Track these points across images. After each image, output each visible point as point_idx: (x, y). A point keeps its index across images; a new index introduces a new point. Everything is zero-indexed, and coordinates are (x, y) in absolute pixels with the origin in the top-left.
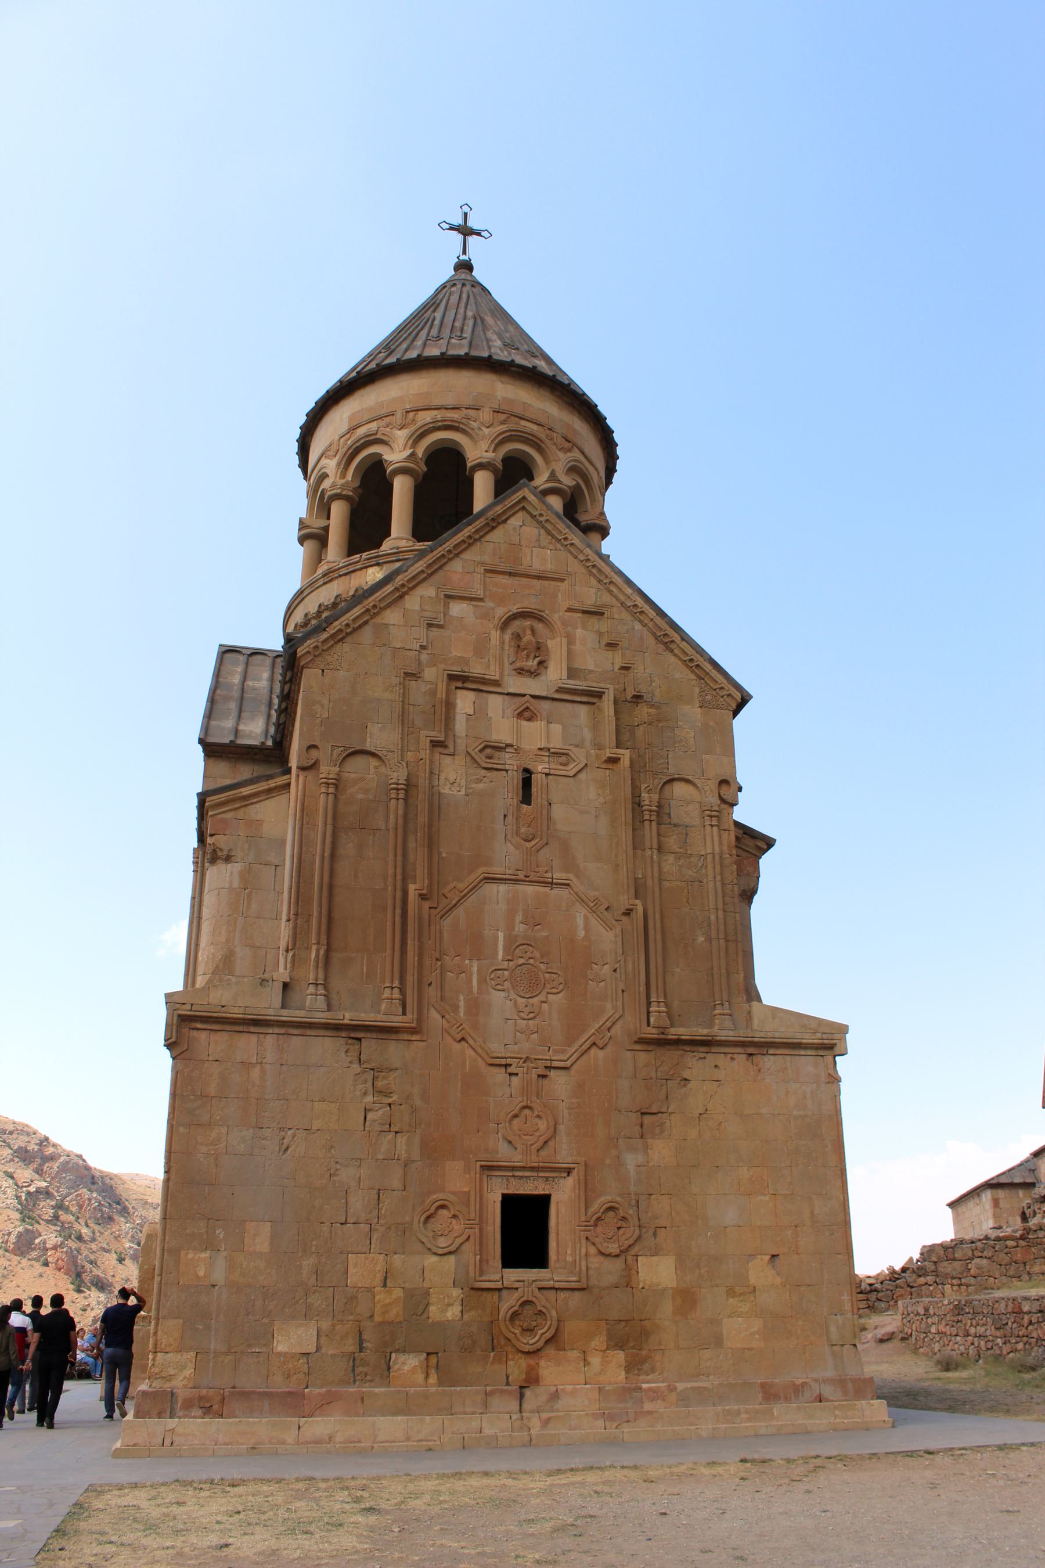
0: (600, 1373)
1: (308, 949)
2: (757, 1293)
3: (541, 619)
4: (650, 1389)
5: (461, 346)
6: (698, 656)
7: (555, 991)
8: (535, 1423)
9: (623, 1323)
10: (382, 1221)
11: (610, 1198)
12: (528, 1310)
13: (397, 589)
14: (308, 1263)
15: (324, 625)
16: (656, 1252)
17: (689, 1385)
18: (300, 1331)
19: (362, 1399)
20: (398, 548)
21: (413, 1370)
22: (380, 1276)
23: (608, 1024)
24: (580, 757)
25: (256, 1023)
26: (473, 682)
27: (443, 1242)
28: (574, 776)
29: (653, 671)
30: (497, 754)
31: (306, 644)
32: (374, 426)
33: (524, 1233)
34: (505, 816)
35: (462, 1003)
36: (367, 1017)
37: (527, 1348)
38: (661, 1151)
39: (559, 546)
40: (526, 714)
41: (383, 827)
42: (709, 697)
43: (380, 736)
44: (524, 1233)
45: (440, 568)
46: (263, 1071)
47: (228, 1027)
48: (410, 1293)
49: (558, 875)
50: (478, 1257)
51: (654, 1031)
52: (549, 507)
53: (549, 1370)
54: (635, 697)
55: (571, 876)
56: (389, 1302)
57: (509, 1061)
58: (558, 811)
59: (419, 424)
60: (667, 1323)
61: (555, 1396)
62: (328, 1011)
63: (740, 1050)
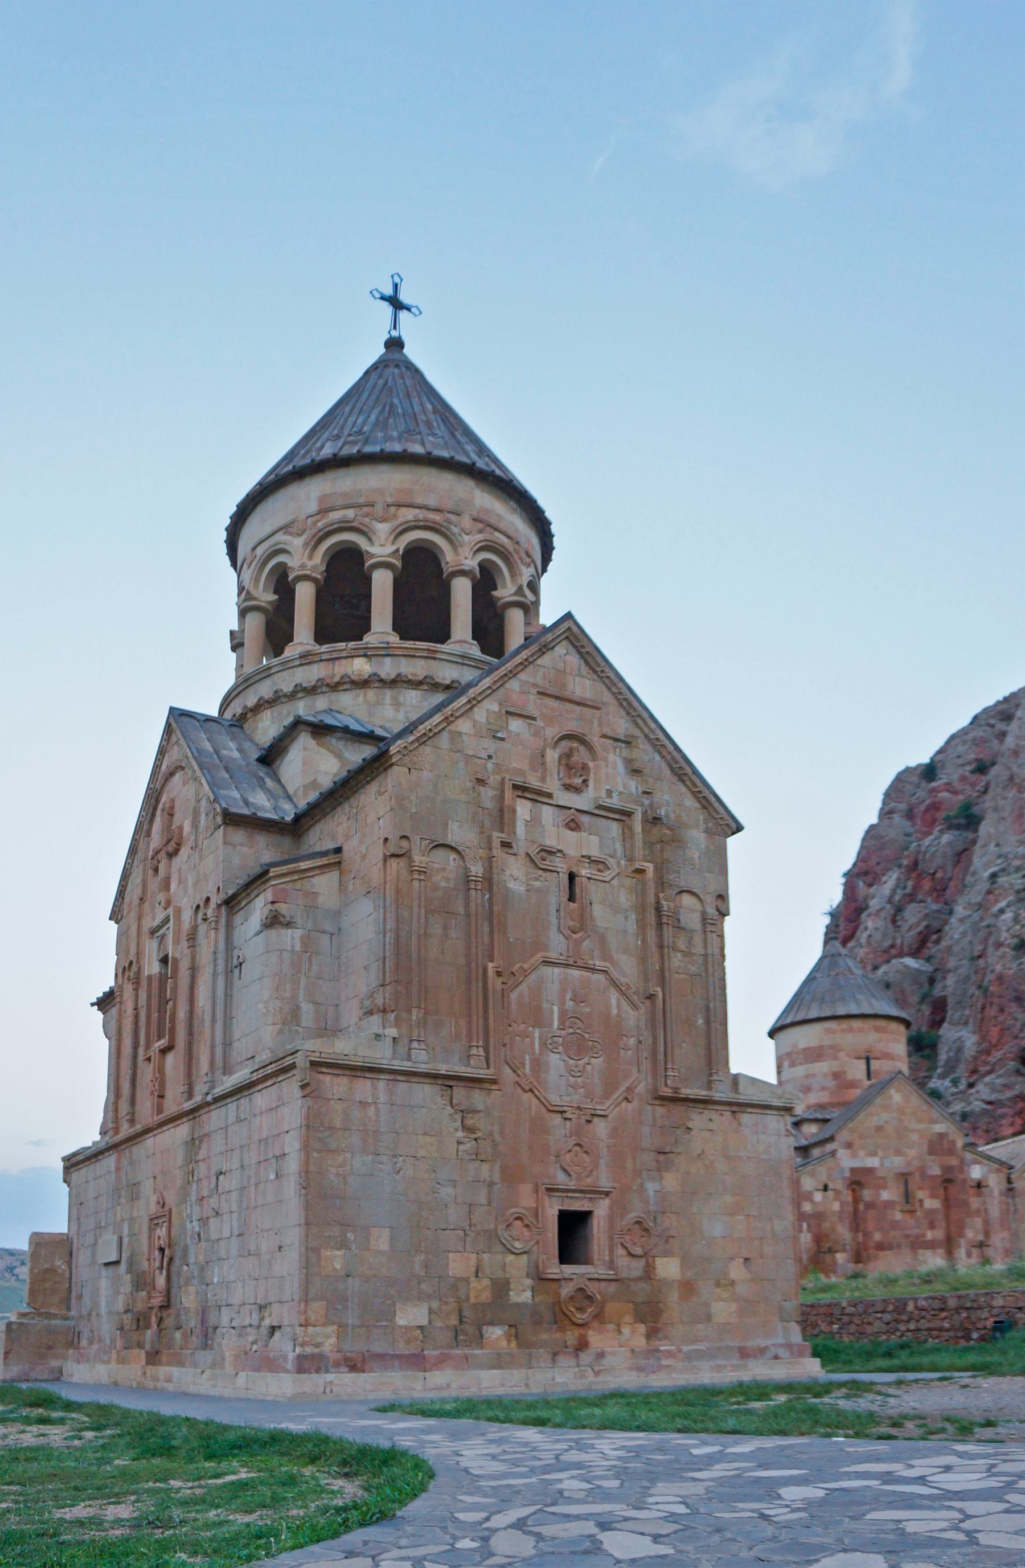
17: (690, 1348)
25: (372, 1070)
26: (531, 792)
29: (671, 799)
35: (527, 1062)
36: (461, 1070)
47: (347, 1072)
53: (595, 1338)
61: (601, 1355)
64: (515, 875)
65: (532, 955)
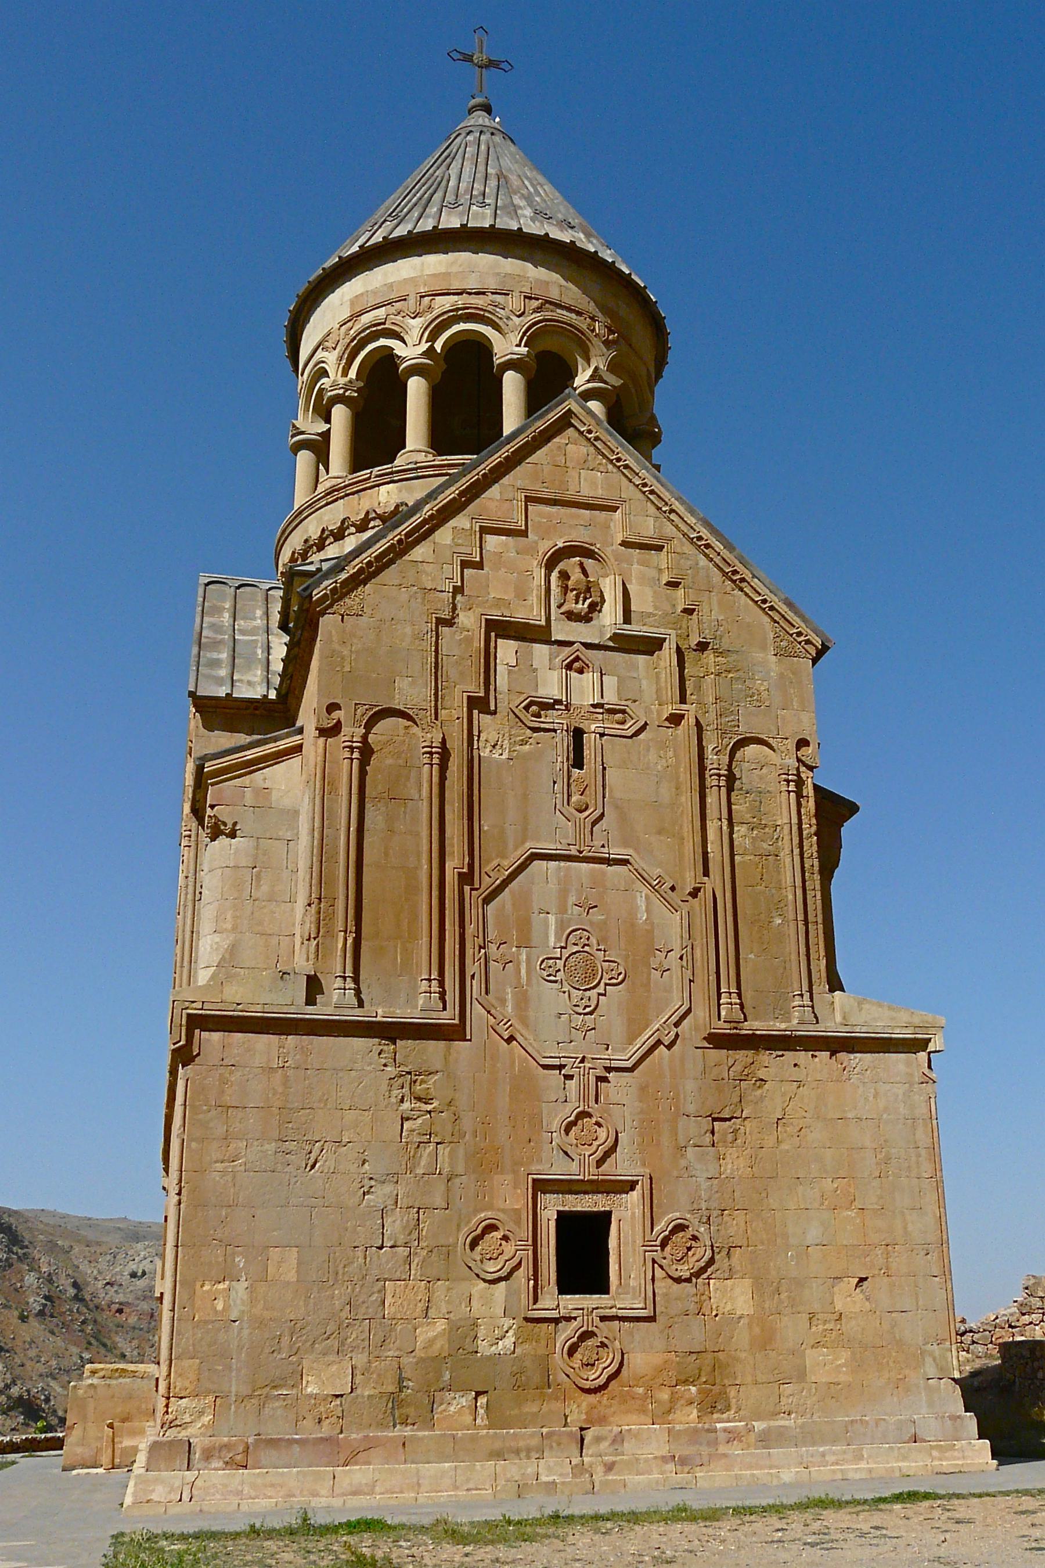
1: (334, 937)
2: (844, 1320)
3: (589, 554)
4: (725, 1430)
5: (484, 217)
6: (772, 596)
7: (614, 981)
9: (694, 1356)
10: (423, 1244)
11: (678, 1215)
13: (425, 522)
15: (343, 563)
19: (404, 1444)
20: (416, 463)
21: (459, 1412)
22: (421, 1306)
24: (639, 714)
27: (492, 1267)
28: (631, 737)
31: (323, 586)
32: (381, 312)
33: (582, 1254)
34: (555, 783)
37: (587, 1385)
38: (735, 1163)
39: (610, 467)
40: (576, 665)
41: (416, 797)
42: (784, 644)
43: (413, 692)
46: (286, 1077)
48: (454, 1328)
49: (616, 852)
50: (532, 1282)
51: (727, 1026)
52: (590, 412)
54: (699, 644)
55: (631, 851)
56: (432, 1333)
57: (564, 1061)
59: (435, 313)
60: (743, 1355)
61: (619, 1439)
62: (359, 1007)
65: (516, 848)
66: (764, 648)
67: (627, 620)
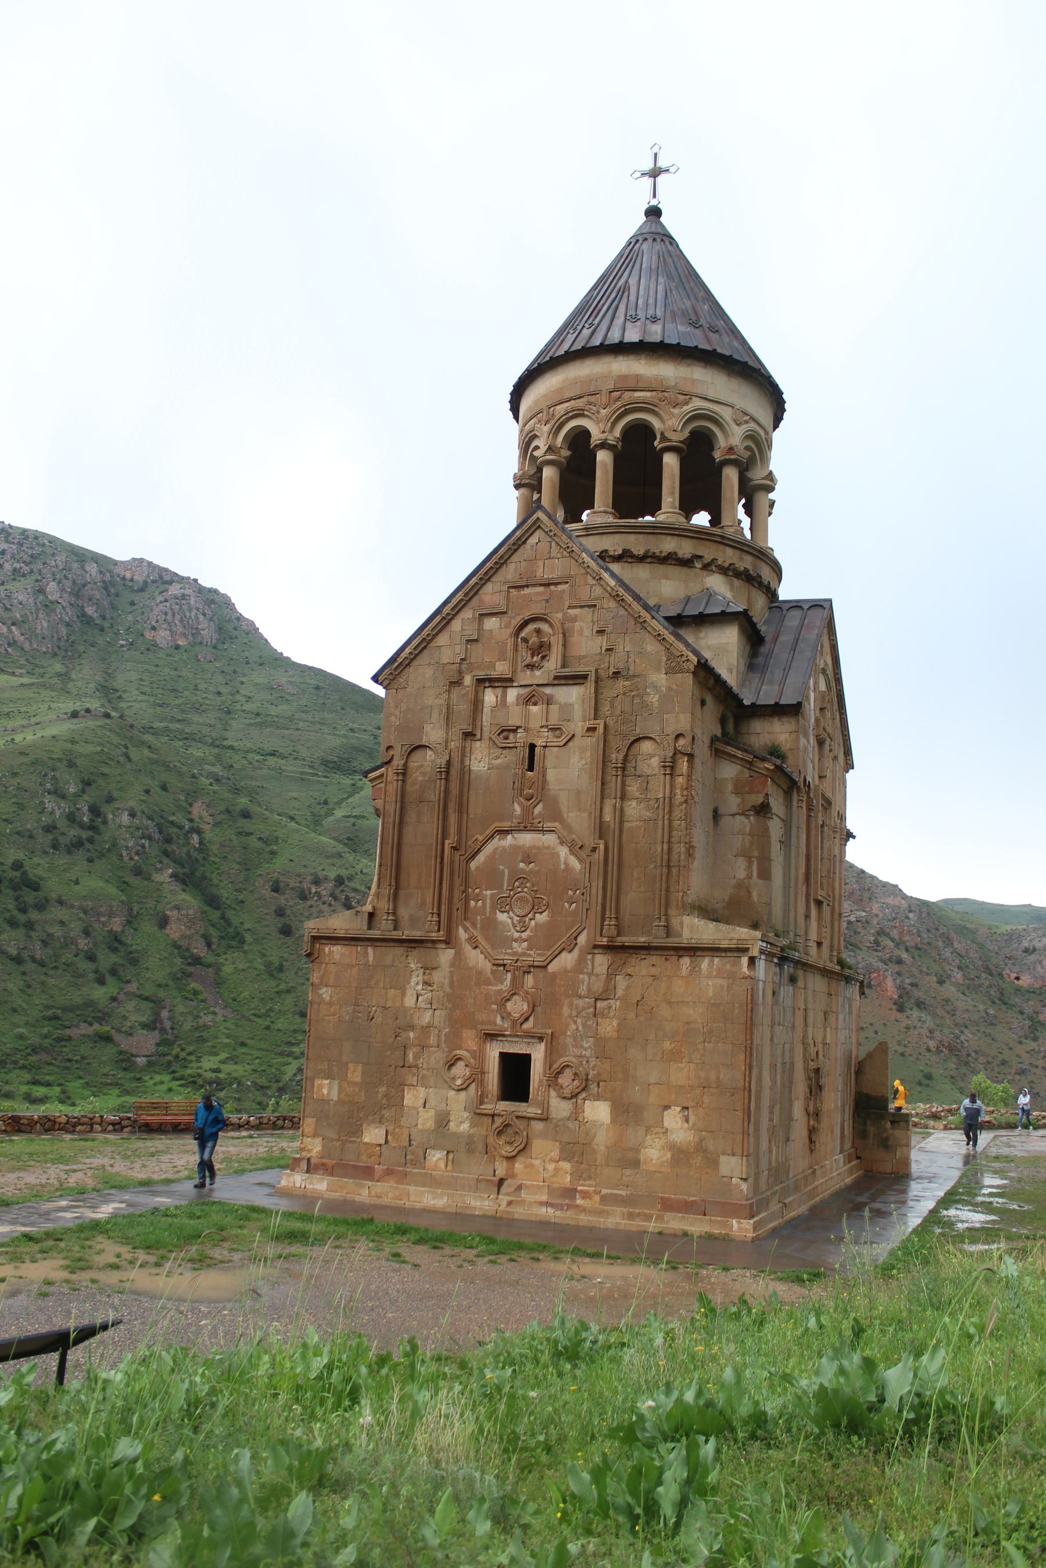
0: (553, 1176)
3: (546, 620)
8: (504, 1204)
12: (510, 1131)
13: (444, 618)
14: (383, 1089)
16: (598, 1098)
18: (377, 1130)
22: (422, 1101)
23: (575, 935)
24: (569, 728)
27: (459, 1082)
30: (511, 735)
33: (515, 1077)
35: (478, 922)
36: (416, 934)
40: (533, 700)
43: (434, 734)
44: (515, 1077)
45: (476, 593)
54: (614, 673)
55: (557, 824)
58: (551, 774)
59: (557, 418)
61: (519, 1188)
62: (395, 929)
63: (672, 952)
64: (481, 760)
66: (658, 669)
67: (563, 666)
